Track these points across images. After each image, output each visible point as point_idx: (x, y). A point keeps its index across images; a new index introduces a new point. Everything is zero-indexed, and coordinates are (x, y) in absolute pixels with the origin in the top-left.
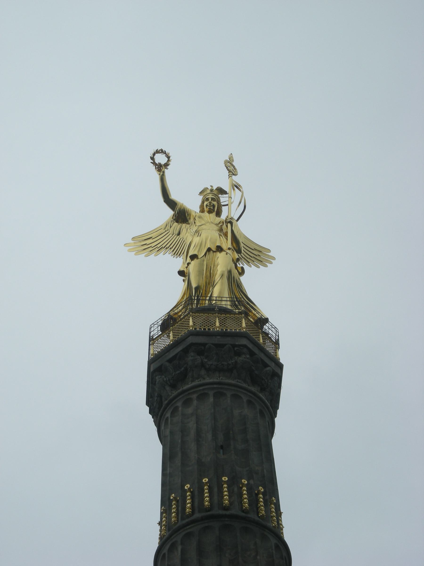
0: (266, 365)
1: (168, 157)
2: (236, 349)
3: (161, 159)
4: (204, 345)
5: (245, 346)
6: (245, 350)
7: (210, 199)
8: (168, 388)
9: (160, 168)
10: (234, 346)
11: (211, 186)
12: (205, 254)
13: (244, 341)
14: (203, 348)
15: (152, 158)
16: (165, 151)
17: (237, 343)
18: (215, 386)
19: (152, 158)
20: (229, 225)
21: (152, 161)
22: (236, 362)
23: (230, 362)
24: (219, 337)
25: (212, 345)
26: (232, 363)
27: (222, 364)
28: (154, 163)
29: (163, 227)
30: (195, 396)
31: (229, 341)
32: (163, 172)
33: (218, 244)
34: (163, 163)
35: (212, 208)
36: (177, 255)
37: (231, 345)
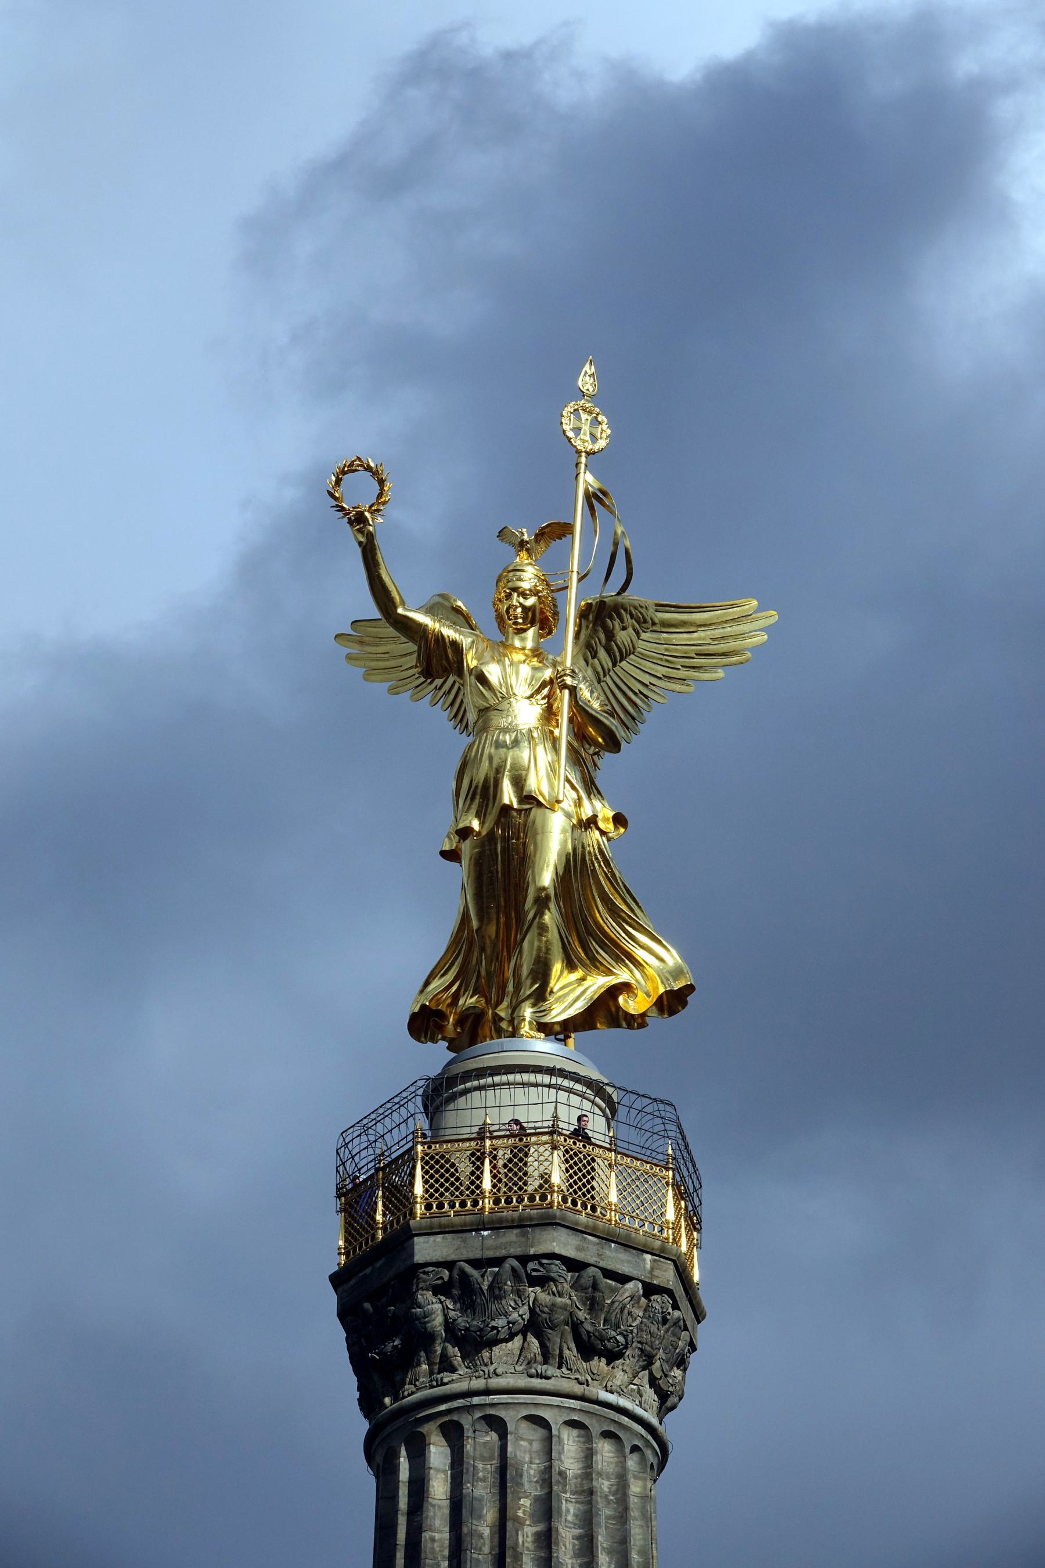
0: (624, 1279)
2: (531, 1265)
3: (359, 492)
4: (449, 1265)
5: (553, 1256)
6: (557, 1268)
9: (359, 520)
10: (524, 1259)
14: (446, 1274)
17: (532, 1252)
18: (476, 1400)
20: (567, 692)
22: (532, 1311)
23: (515, 1316)
24: (486, 1233)
25: (468, 1269)
26: (521, 1316)
27: (494, 1328)
31: (510, 1242)
35: (520, 621)
37: (517, 1258)
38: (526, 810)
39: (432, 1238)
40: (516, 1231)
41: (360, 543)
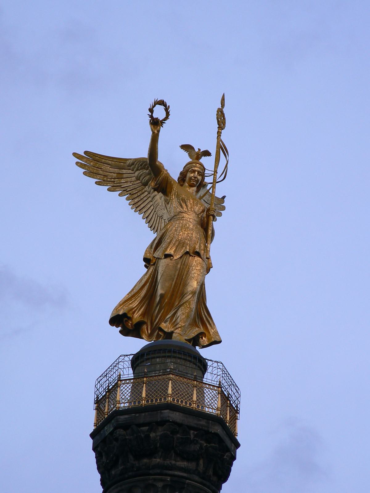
1: (168, 114)
3: (159, 112)
4: (180, 425)
5: (216, 435)
7: (196, 173)
8: (131, 457)
9: (156, 123)
11: (199, 150)
12: (181, 257)
13: (217, 429)
15: (151, 110)
16: (166, 104)
19: (151, 110)
20: (212, 217)
21: (150, 114)
28: (151, 116)
29: (128, 162)
30: (160, 485)
32: (159, 131)
33: (198, 250)
34: (161, 118)
36: (136, 208)
38: (192, 256)
39: (175, 413)
40: (205, 420)
41: (153, 133)
